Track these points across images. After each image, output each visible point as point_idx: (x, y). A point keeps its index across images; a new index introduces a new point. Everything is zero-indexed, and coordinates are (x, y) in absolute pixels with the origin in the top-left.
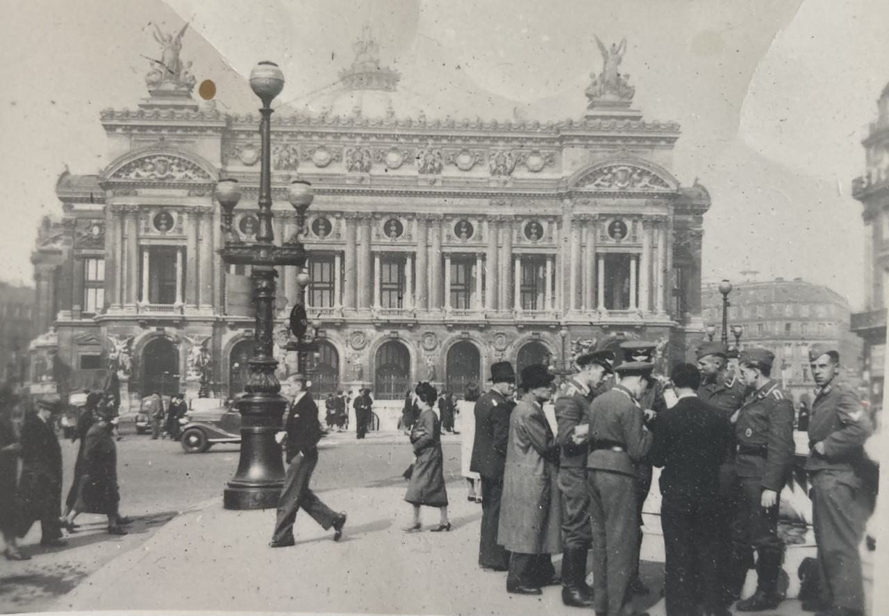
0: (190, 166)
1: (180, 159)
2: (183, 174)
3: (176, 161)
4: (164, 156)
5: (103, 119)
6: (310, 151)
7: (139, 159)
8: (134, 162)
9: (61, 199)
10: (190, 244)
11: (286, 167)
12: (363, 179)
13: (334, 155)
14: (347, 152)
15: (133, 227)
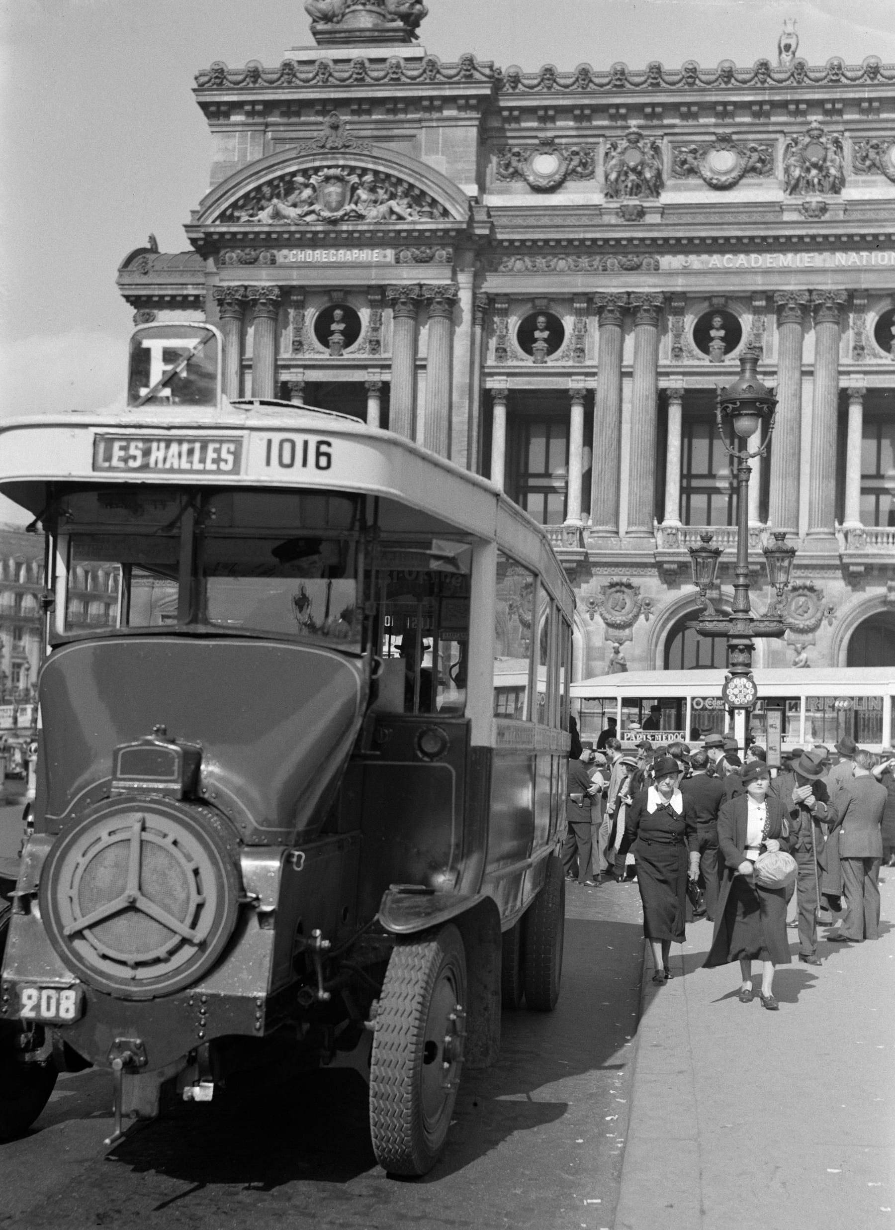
0: (400, 189)
1: (376, 173)
2: (383, 208)
3: (369, 178)
4: (337, 166)
5: (199, 90)
6: (694, 151)
7: (281, 178)
8: (270, 183)
9: (127, 298)
10: (399, 378)
11: (636, 190)
12: (824, 209)
13: (755, 156)
14: (788, 146)
15: (267, 341)
